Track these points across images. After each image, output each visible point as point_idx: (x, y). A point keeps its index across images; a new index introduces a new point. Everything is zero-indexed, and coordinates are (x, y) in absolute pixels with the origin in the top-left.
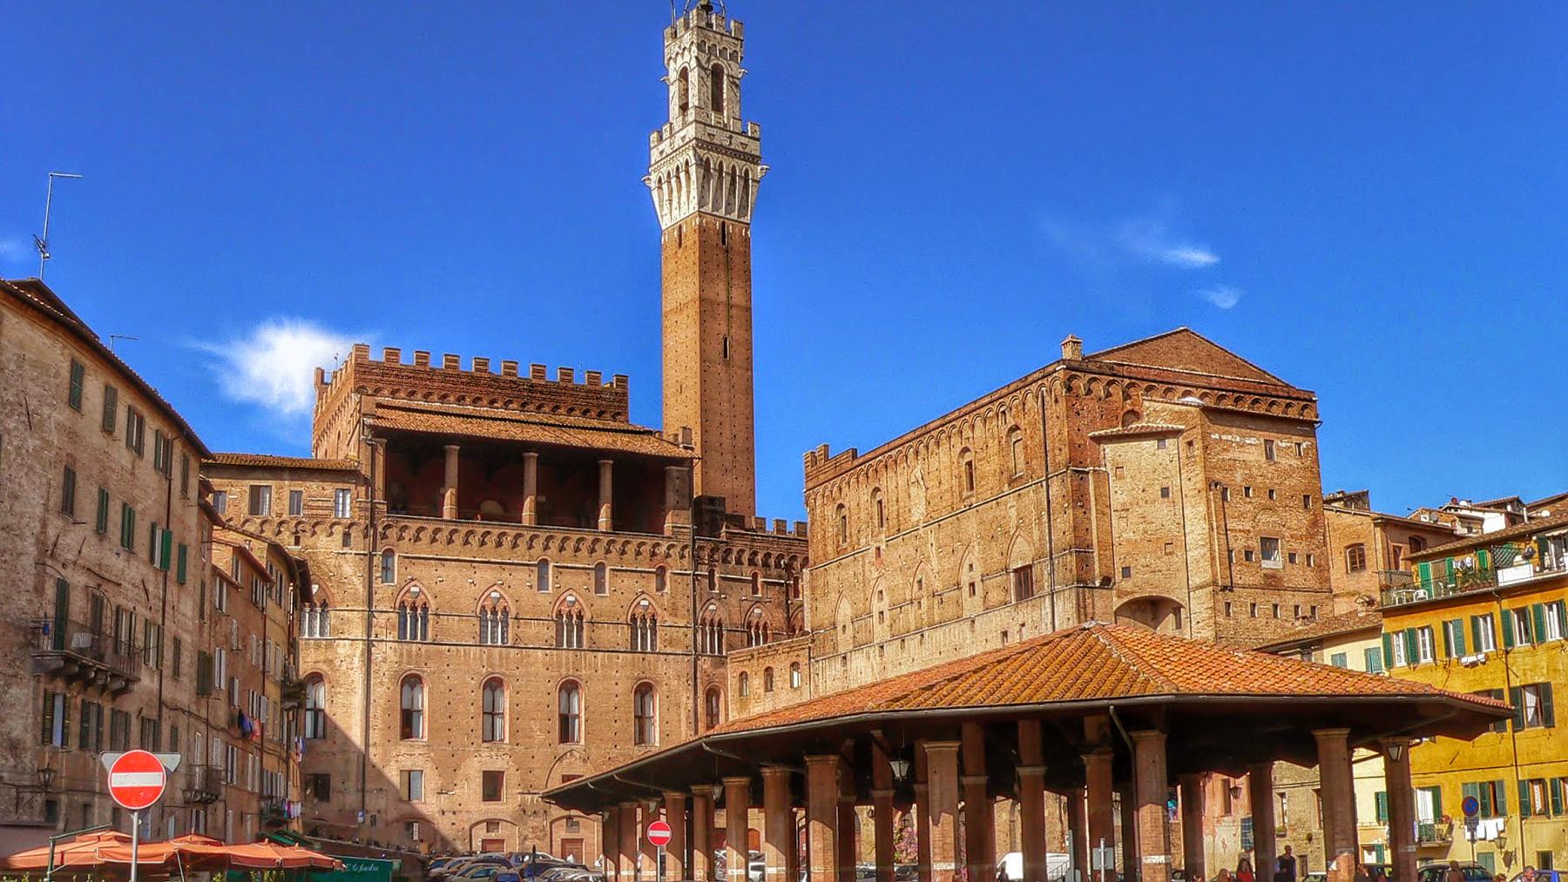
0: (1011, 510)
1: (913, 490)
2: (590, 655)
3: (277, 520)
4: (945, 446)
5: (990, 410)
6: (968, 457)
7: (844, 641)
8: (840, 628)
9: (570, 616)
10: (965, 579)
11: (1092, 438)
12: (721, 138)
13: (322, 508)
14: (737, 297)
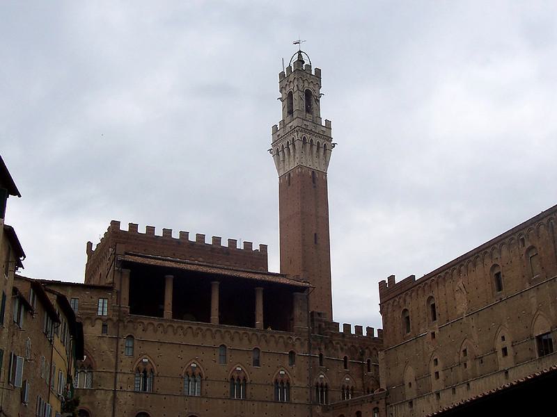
1: (458, 295)
2: (250, 403)
4: (480, 266)
5: (513, 239)
7: (410, 393)
9: (238, 379)
10: (499, 346)
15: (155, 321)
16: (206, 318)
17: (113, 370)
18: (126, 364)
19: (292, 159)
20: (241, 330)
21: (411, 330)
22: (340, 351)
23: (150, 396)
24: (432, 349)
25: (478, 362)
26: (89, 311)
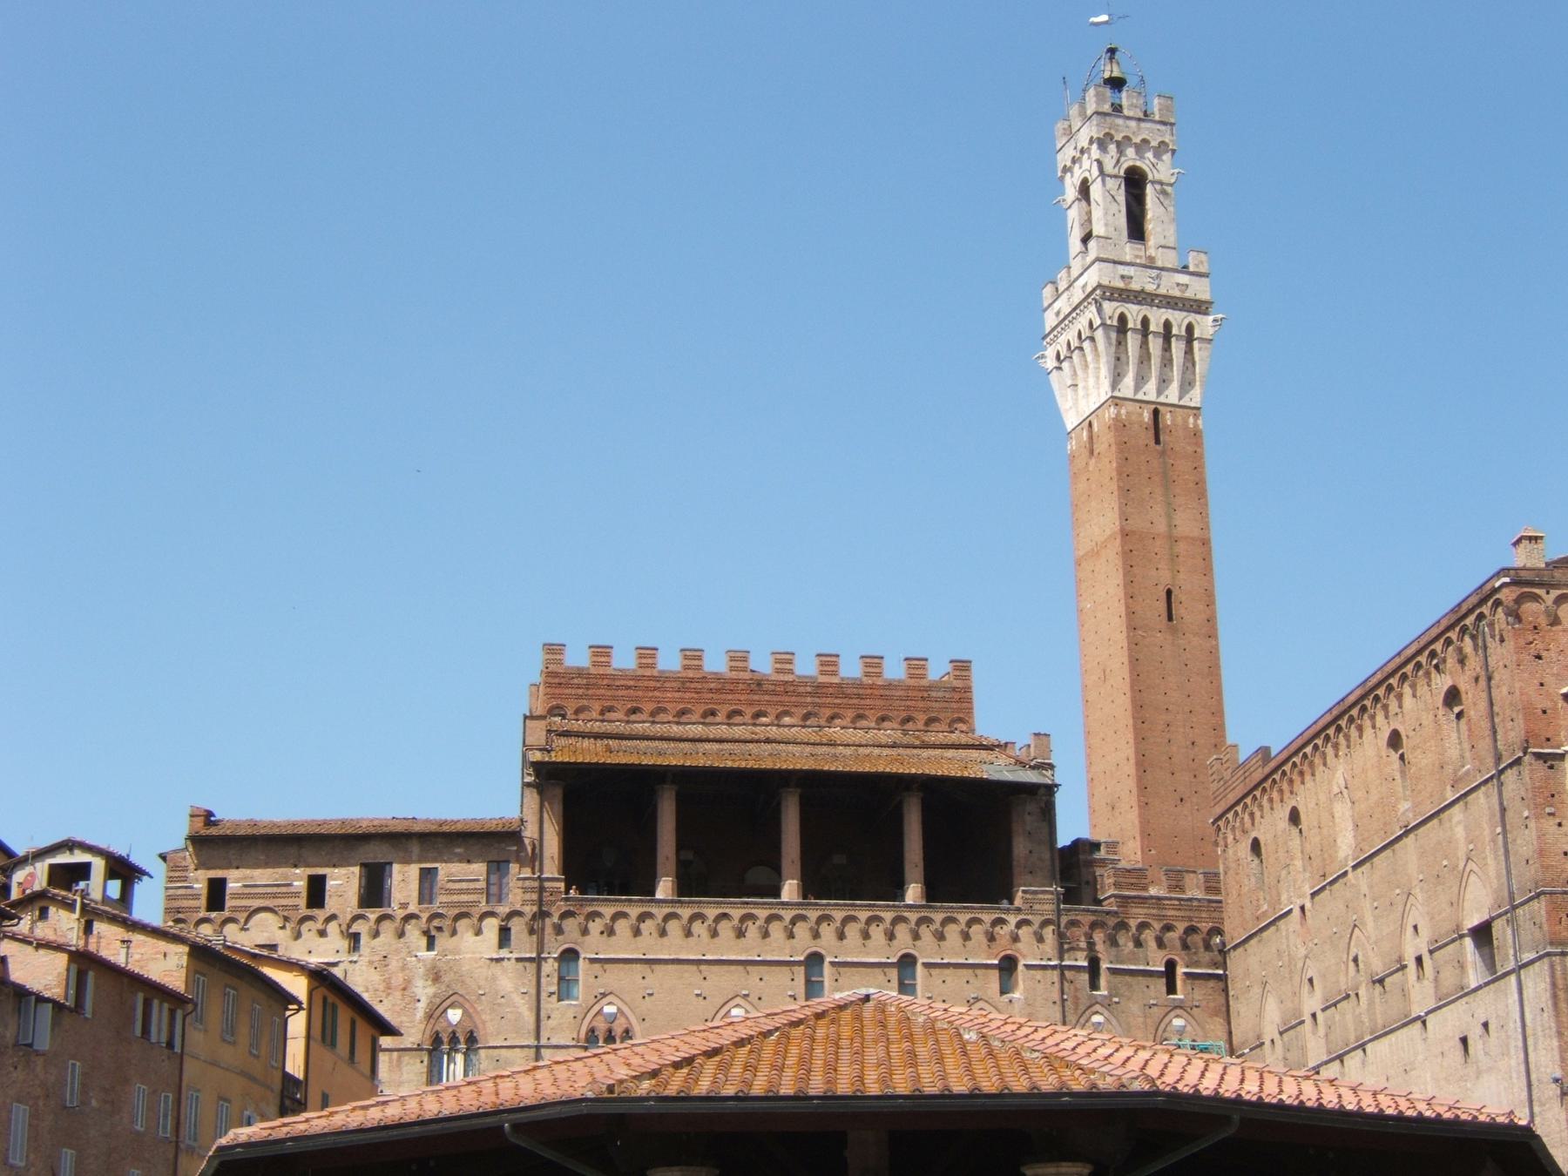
3: (400, 914)
8: (1268, 1043)
12: (1142, 281)
13: (467, 892)
14: (1185, 524)
22: (1153, 944)
24: (1302, 951)
26: (464, 898)
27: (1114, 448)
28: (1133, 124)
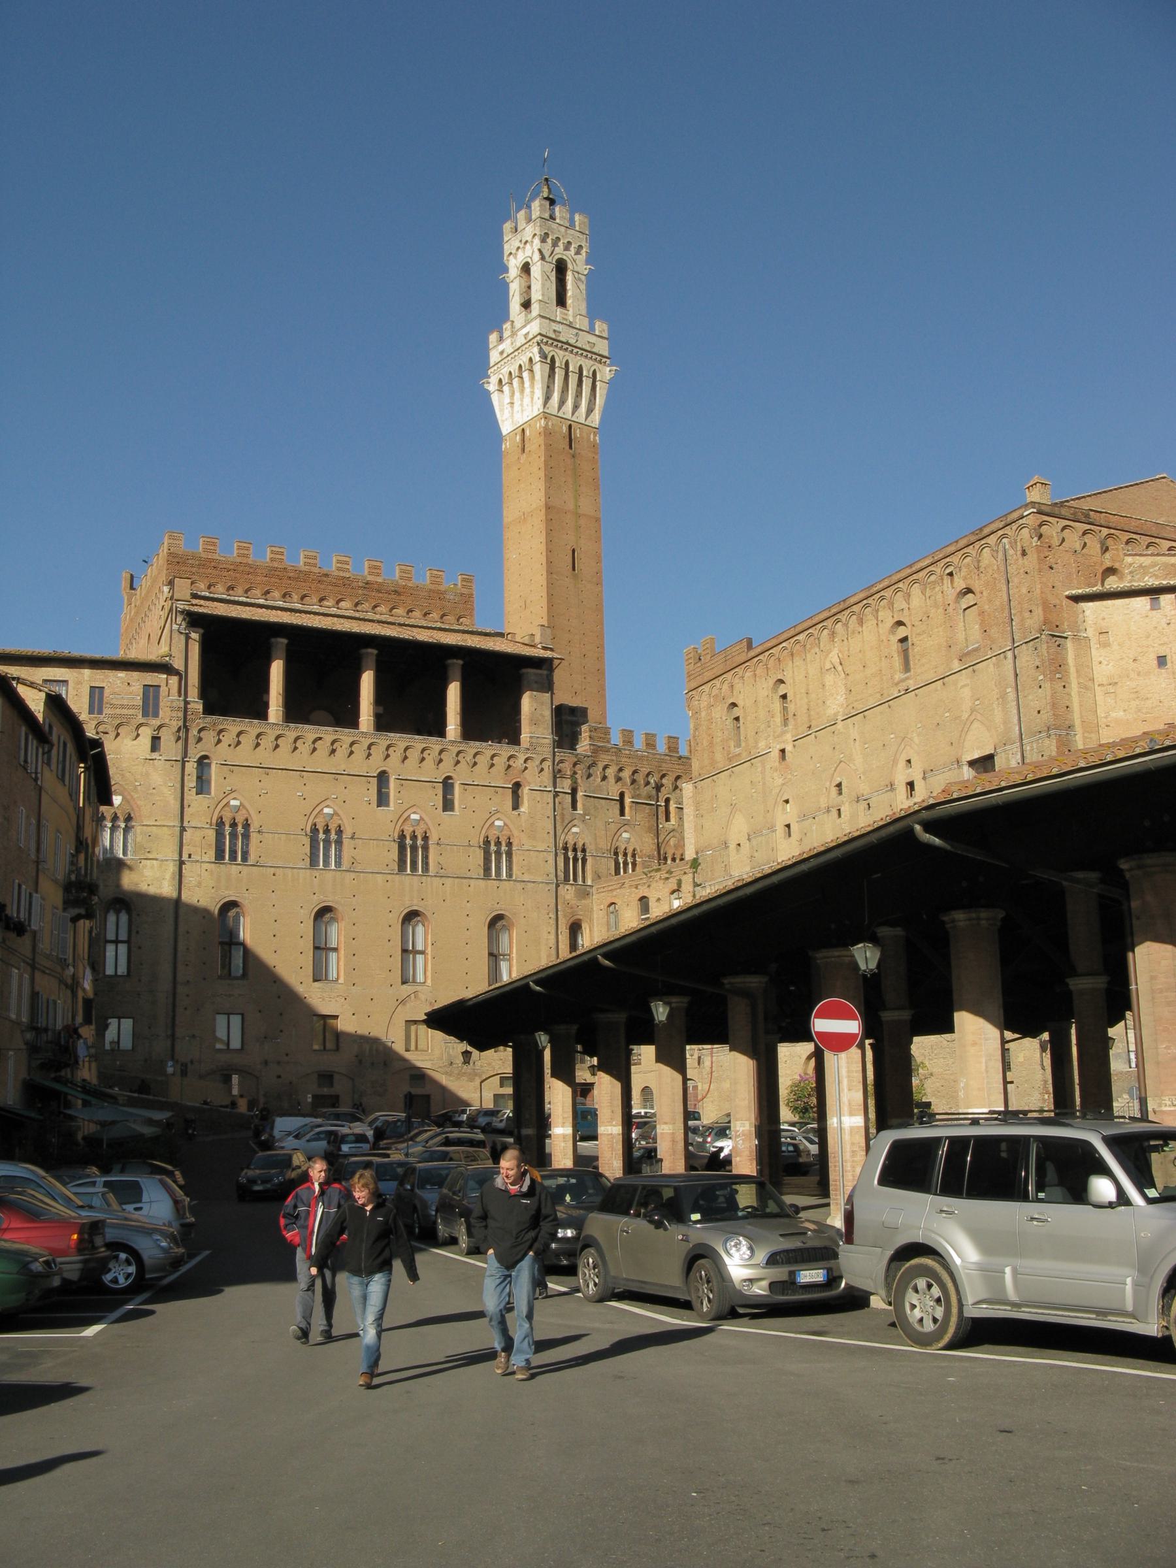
0: (964, 688)
1: (829, 679)
4: (870, 623)
5: (932, 573)
6: (902, 632)
8: (732, 846)
11: (1068, 597)
12: (567, 335)
14: (586, 506)
15: (252, 727)
16: (349, 719)
17: (178, 823)
18: (200, 809)
19: (527, 400)
20: (418, 742)
21: (743, 744)
23: (245, 870)
24: (781, 781)
25: (863, 805)
26: (125, 711)
27: (543, 447)
28: (563, 229)
